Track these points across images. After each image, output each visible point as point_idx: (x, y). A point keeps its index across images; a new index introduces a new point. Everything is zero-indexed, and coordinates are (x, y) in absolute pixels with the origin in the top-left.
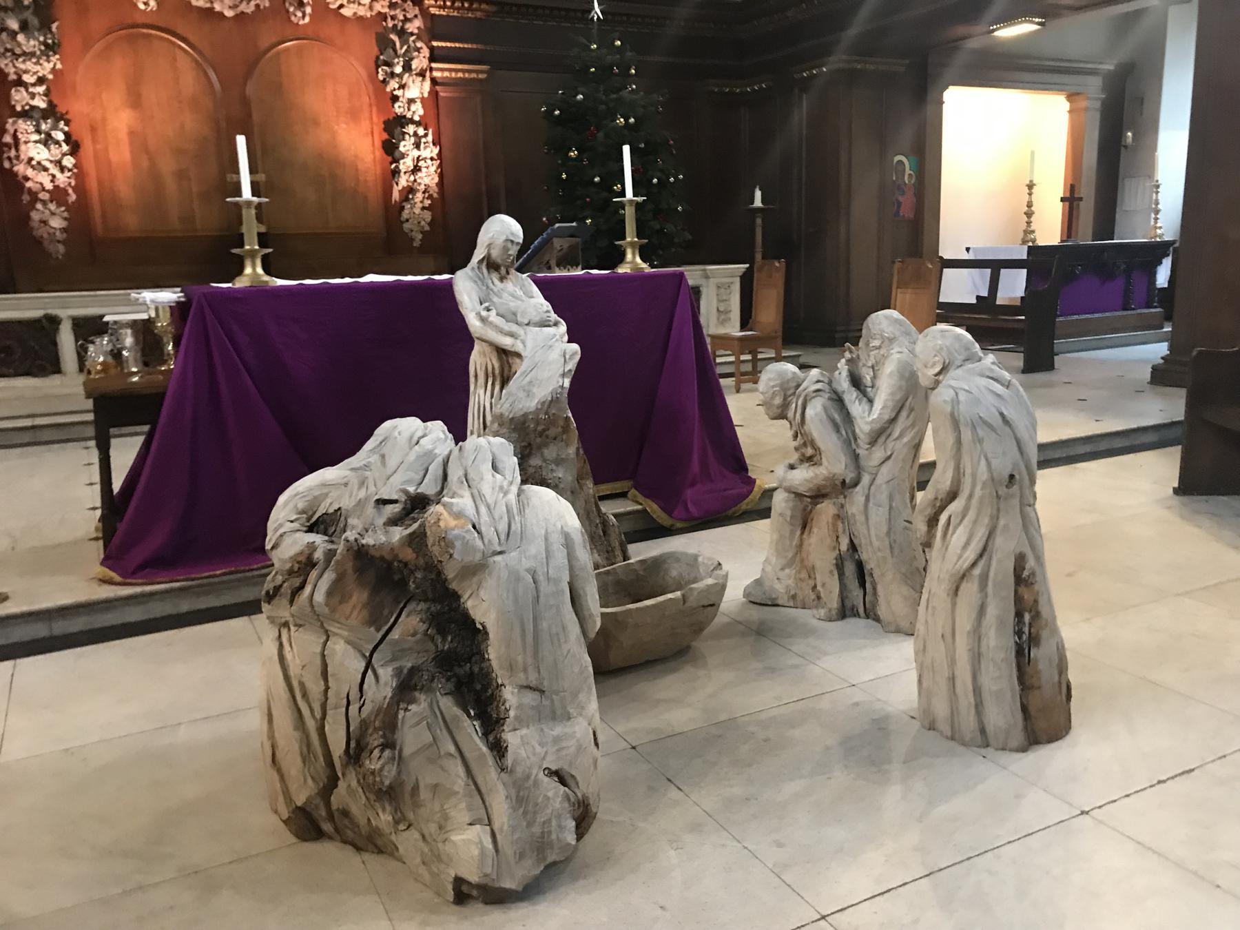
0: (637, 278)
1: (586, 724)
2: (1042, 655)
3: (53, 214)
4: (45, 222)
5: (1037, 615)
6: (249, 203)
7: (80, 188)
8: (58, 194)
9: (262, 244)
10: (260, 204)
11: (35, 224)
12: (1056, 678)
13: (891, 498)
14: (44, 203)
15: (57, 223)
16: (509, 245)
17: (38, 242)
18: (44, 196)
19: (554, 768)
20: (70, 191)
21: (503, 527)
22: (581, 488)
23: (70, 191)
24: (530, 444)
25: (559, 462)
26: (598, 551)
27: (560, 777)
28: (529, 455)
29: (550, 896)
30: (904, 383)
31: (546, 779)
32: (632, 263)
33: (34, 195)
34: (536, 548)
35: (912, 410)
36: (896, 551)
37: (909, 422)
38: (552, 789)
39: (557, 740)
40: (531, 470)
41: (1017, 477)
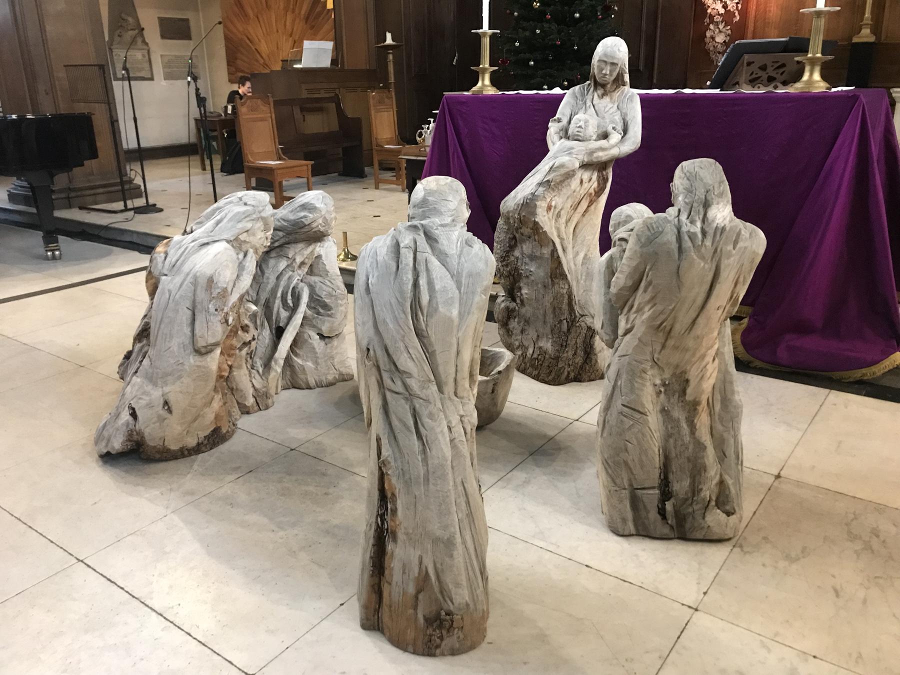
0: (808, 100)
1: (161, 393)
2: (401, 554)
3: (720, 32)
4: (713, 38)
5: (394, 511)
6: (485, 34)
7: (744, 13)
8: (728, 16)
9: (491, 65)
10: (494, 33)
11: (707, 40)
12: (411, 589)
13: (618, 375)
14: (717, 24)
15: (720, 39)
16: (603, 65)
17: (707, 52)
18: (718, 19)
19: (133, 406)
20: (737, 14)
21: (174, 260)
22: (553, 284)
23: (737, 14)
24: (514, 238)
25: (533, 258)
26: (554, 342)
27: (134, 414)
28: (515, 245)
29: (117, 470)
30: (637, 248)
31: (127, 409)
32: (813, 81)
33: (711, 17)
34: (178, 280)
35: (649, 284)
36: (605, 435)
37: (648, 296)
38: (126, 416)
39: (144, 393)
40: (512, 258)
41: (371, 352)
